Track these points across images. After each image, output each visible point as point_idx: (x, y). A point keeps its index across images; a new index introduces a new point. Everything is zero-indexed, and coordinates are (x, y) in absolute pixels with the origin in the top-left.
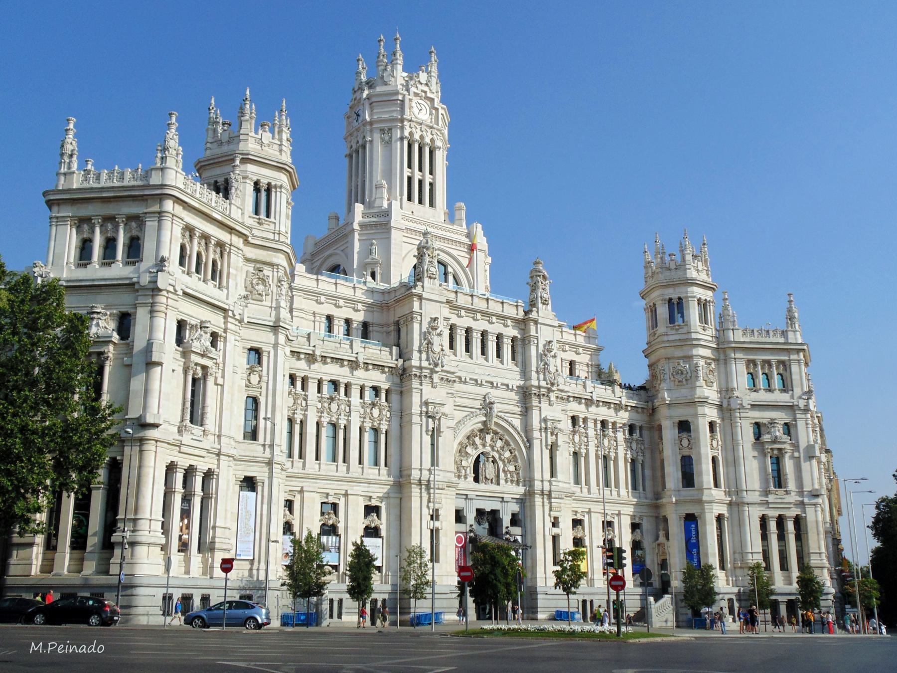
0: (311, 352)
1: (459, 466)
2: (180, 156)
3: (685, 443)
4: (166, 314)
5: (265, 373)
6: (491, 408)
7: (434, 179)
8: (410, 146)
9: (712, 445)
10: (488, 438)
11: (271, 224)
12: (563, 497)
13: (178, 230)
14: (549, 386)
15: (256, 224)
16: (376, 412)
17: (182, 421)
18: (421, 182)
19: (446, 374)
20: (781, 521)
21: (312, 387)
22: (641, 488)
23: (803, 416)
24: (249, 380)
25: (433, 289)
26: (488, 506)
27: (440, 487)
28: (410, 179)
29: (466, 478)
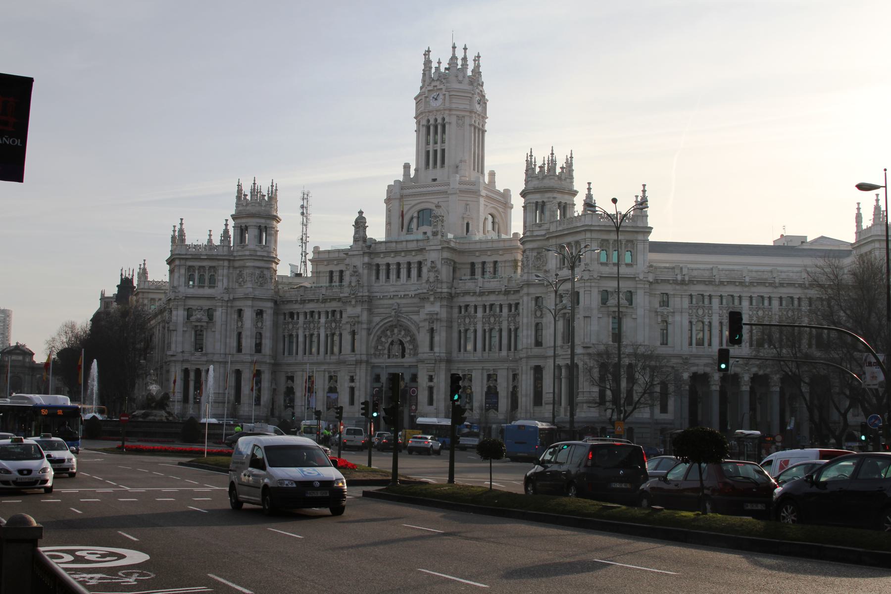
1: (376, 348)
4: (177, 309)
5: (244, 320)
8: (428, 128)
9: (536, 315)
10: (396, 331)
12: (433, 362)
13: (183, 271)
14: (429, 292)
16: (333, 325)
18: (435, 152)
21: (302, 318)
23: (583, 285)
24: (237, 325)
27: (352, 364)
28: (428, 152)
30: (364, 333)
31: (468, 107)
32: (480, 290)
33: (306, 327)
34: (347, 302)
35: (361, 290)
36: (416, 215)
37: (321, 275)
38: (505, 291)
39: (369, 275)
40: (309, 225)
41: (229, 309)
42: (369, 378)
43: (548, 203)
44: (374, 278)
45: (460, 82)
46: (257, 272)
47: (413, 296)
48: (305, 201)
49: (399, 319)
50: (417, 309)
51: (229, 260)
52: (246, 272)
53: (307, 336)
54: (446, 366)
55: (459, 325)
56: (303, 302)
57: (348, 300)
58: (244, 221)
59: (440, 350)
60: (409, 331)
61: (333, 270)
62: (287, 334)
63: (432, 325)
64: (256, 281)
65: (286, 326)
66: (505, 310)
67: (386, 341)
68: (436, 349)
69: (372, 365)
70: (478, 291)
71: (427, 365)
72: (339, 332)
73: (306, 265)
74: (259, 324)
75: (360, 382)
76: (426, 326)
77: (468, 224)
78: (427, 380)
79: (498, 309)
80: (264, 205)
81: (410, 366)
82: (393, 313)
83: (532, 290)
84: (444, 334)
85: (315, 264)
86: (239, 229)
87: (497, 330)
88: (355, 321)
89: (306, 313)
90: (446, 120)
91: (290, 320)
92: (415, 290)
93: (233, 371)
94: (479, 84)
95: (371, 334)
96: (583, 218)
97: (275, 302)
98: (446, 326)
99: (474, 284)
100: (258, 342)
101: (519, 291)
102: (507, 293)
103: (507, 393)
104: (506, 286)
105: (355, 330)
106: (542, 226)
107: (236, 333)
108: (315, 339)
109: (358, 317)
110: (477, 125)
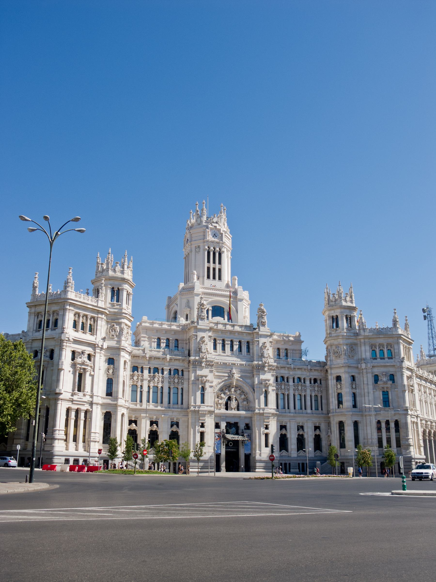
2: (73, 285)
3: (339, 386)
6: (233, 376)
7: (221, 267)
8: (209, 253)
9: (352, 387)
10: (233, 390)
16: (176, 380)
17: (73, 390)
18: (214, 269)
20: (387, 423)
21: (146, 372)
22: (320, 409)
25: (203, 323)
26: (232, 421)
27: (204, 413)
28: (209, 268)
36: (211, 308)
47: (247, 365)
58: (116, 283)
66: (308, 382)
79: (303, 381)
90: (223, 249)
96: (394, 329)
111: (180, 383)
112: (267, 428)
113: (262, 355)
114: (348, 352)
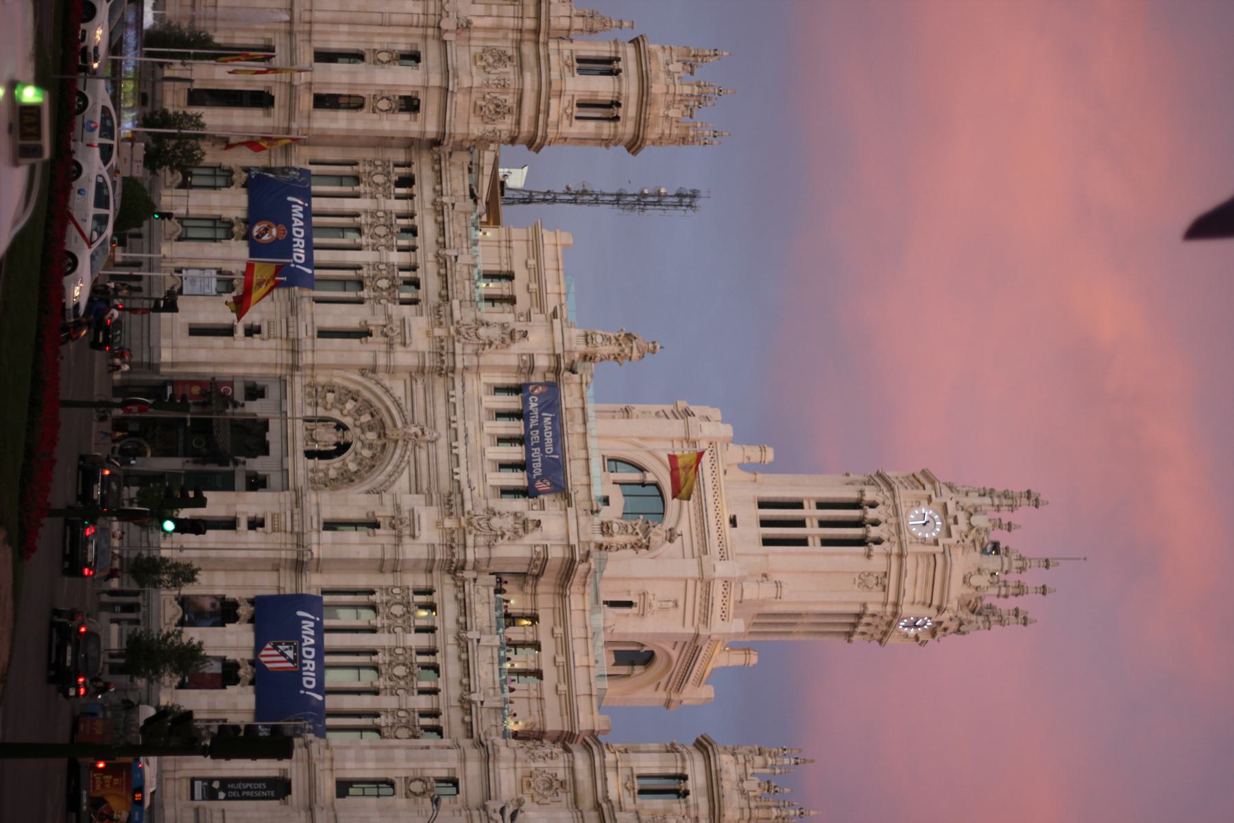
0: (444, 193)
5: (393, 67)
8: (856, 505)
10: (371, 436)
11: (571, 74)
12: (296, 529)
14: (466, 516)
15: (565, 58)
16: (384, 283)
18: (801, 523)
19: (451, 350)
21: (400, 206)
24: (382, 52)
26: (273, 436)
27: (291, 330)
28: (798, 505)
29: (310, 404)
30: (365, 358)
31: (907, 598)
32: (472, 640)
33: (378, 217)
34: (441, 316)
35: (469, 349)
36: (650, 478)
37: (504, 251)
38: (470, 702)
39: (504, 369)
40: (616, 210)
41: (420, 31)
42: (256, 371)
43: (683, 805)
44: (499, 380)
45: (964, 582)
46: (511, 100)
47: (456, 477)
48: (676, 200)
49: (401, 443)
50: (424, 484)
51: (537, 31)
52: (510, 71)
53: (357, 219)
54: (286, 559)
55: (387, 590)
56: (439, 209)
57: (443, 320)
59: (323, 544)
60: (374, 466)
61: (516, 281)
62: (361, 170)
63: (387, 522)
64: (488, 97)
65: (380, 168)
66: (424, 702)
67: (345, 412)
68: (328, 536)
69: (288, 378)
70: (470, 635)
71: (289, 514)
72: (366, 296)
73: (524, 203)
74: (383, 105)
75: (246, 349)
76: (383, 512)
77: (629, 604)
78: (252, 514)
79: (424, 684)
80: (670, 115)
81: (287, 470)
82: (413, 430)
83: (472, 771)
84: (364, 553)
85: (531, 239)
86: (613, 55)
87: (376, 684)
88: (395, 336)
89: (411, 216)
90: (876, 548)
91: (395, 178)
92: (469, 481)
93: (270, 40)
94: (961, 624)
95: (363, 375)
97: (436, 143)
98: (383, 560)
99: (486, 624)
100: (342, 101)
101: (472, 737)
102: (466, 705)
103: (220, 711)
104: (482, 703)
105: (371, 335)
106: (629, 790)
107: (362, 47)
108: (350, 239)
109: (404, 344)
110: (865, 620)
111: (377, 294)
112: (255, 524)
113: (495, 514)
114: (541, 770)
